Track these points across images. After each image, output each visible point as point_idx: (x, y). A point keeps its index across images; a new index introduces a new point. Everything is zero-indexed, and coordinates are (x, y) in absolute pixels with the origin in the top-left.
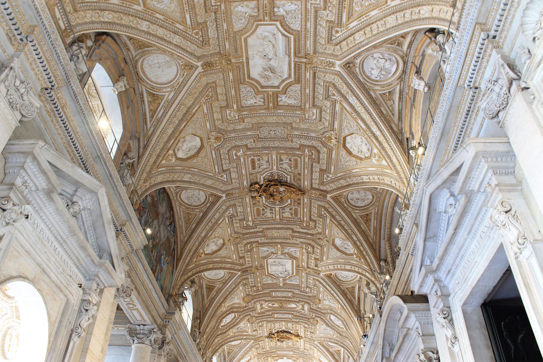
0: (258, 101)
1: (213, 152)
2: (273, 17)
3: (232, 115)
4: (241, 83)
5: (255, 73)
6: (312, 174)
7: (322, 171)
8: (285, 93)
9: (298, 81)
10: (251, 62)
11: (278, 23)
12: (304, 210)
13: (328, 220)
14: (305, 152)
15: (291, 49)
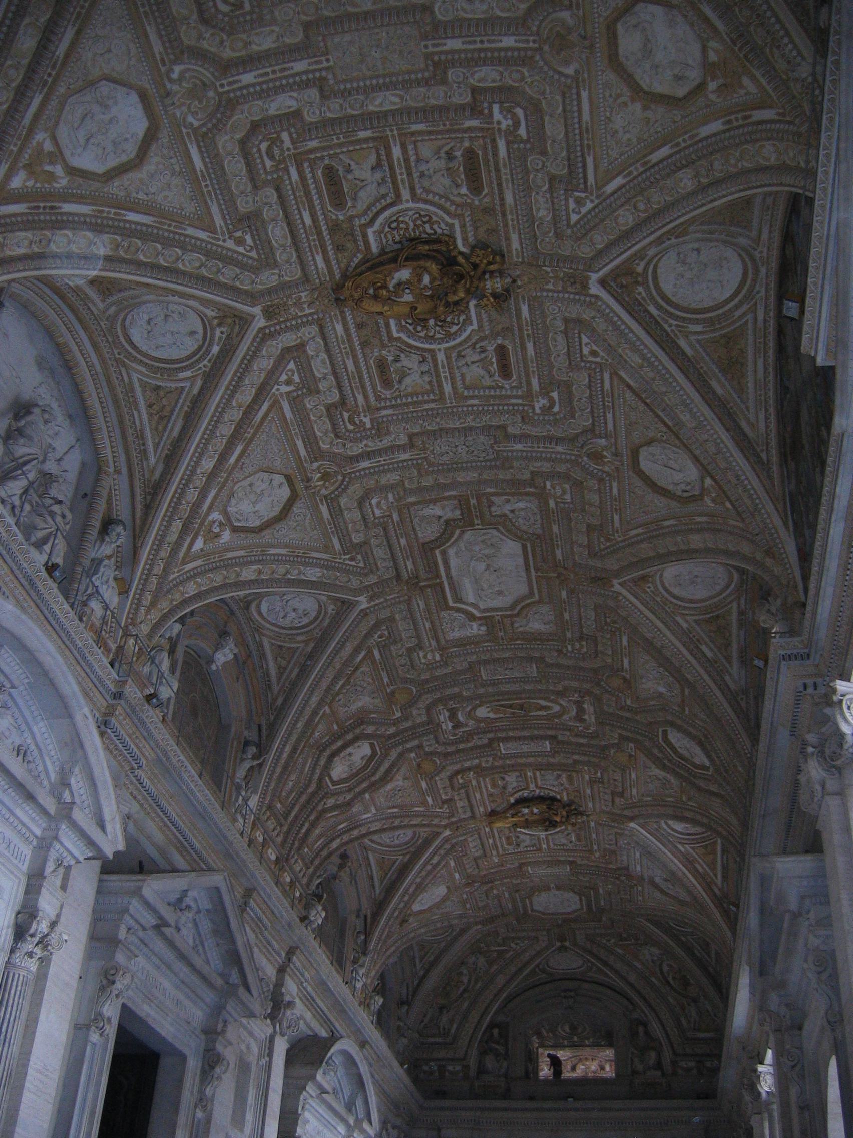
0: (502, 506)
1: (610, 426)
2: (486, 620)
3: (559, 491)
4: (538, 537)
5: (512, 547)
6: (333, 365)
7: (310, 386)
8: (447, 522)
9: (427, 549)
10: (521, 561)
11: (478, 614)
12: (313, 216)
13: (218, 221)
14: (372, 420)
15: (450, 588)
